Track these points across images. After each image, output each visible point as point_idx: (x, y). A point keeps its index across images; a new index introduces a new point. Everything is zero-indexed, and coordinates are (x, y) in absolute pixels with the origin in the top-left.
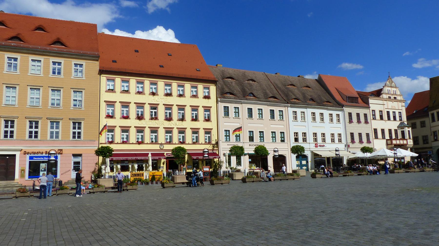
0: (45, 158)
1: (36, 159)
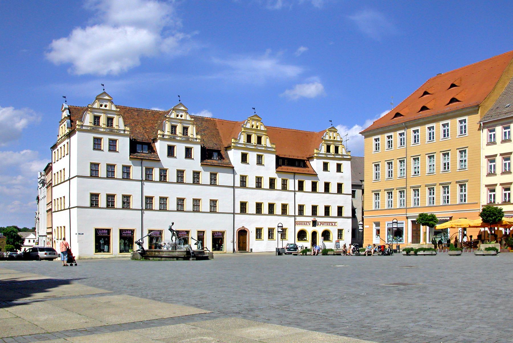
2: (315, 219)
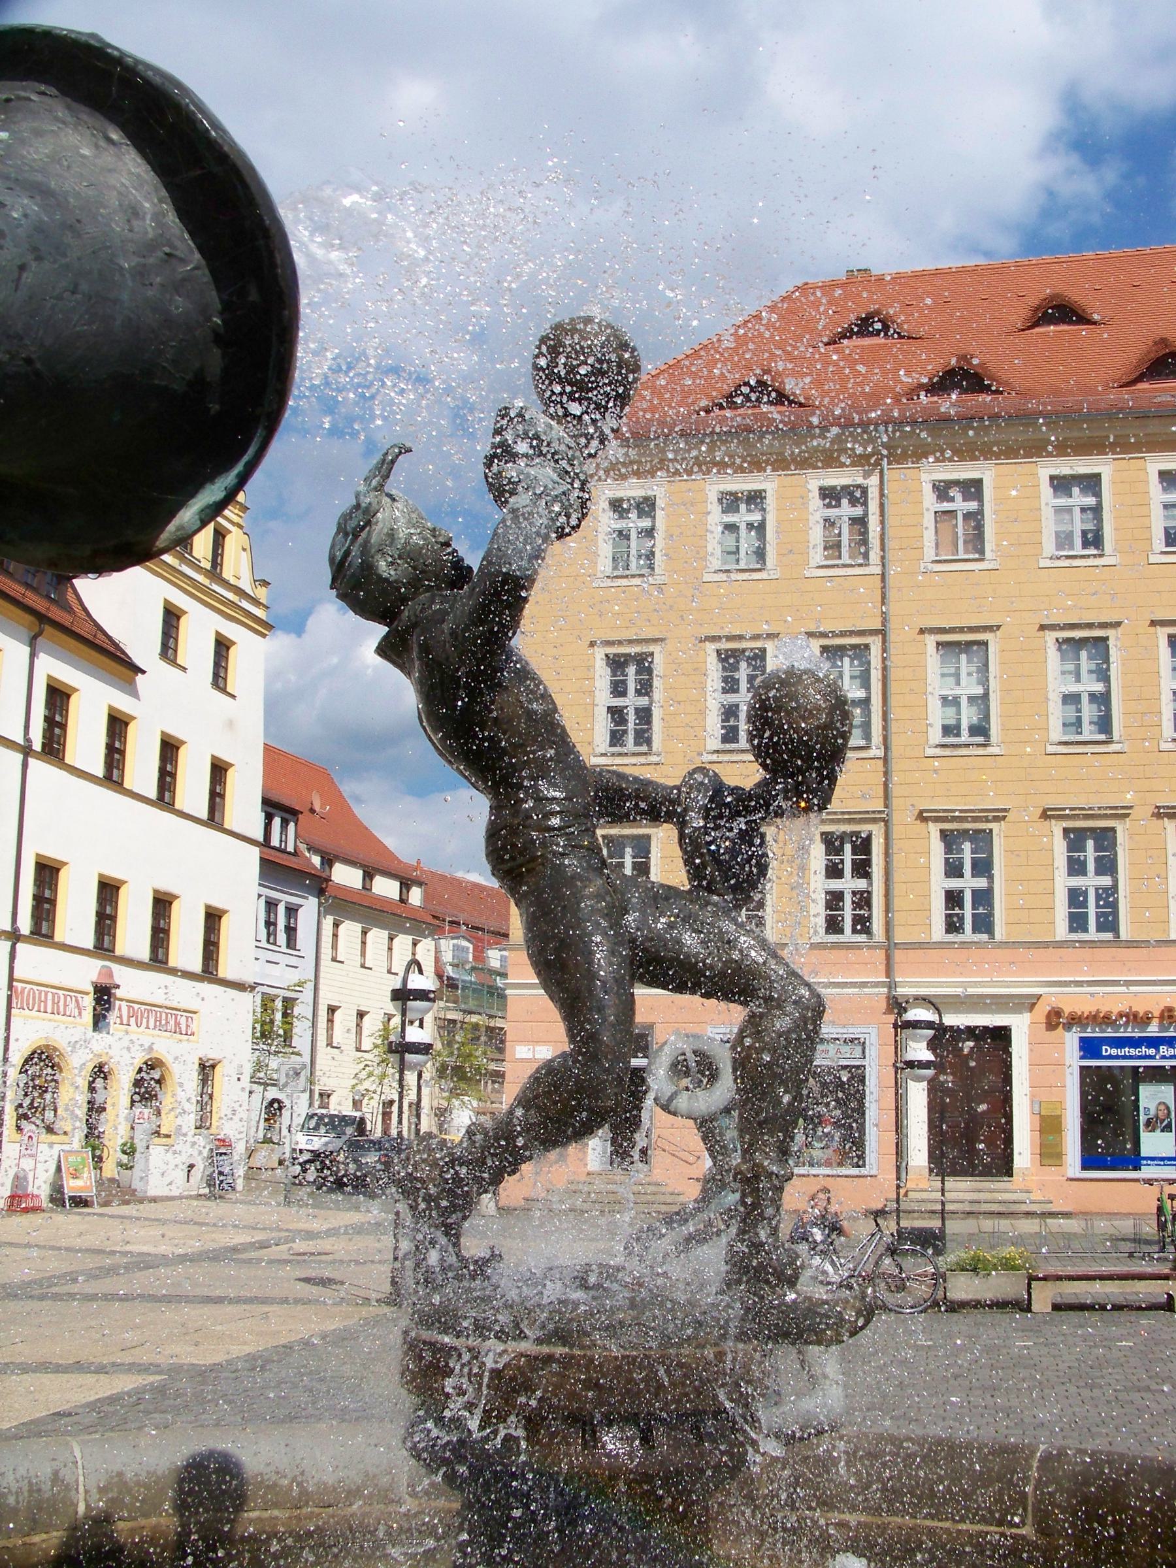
0: (1163, 1049)
1: (1117, 1057)
2: (111, 975)
